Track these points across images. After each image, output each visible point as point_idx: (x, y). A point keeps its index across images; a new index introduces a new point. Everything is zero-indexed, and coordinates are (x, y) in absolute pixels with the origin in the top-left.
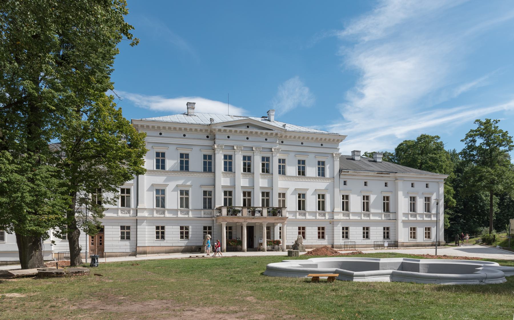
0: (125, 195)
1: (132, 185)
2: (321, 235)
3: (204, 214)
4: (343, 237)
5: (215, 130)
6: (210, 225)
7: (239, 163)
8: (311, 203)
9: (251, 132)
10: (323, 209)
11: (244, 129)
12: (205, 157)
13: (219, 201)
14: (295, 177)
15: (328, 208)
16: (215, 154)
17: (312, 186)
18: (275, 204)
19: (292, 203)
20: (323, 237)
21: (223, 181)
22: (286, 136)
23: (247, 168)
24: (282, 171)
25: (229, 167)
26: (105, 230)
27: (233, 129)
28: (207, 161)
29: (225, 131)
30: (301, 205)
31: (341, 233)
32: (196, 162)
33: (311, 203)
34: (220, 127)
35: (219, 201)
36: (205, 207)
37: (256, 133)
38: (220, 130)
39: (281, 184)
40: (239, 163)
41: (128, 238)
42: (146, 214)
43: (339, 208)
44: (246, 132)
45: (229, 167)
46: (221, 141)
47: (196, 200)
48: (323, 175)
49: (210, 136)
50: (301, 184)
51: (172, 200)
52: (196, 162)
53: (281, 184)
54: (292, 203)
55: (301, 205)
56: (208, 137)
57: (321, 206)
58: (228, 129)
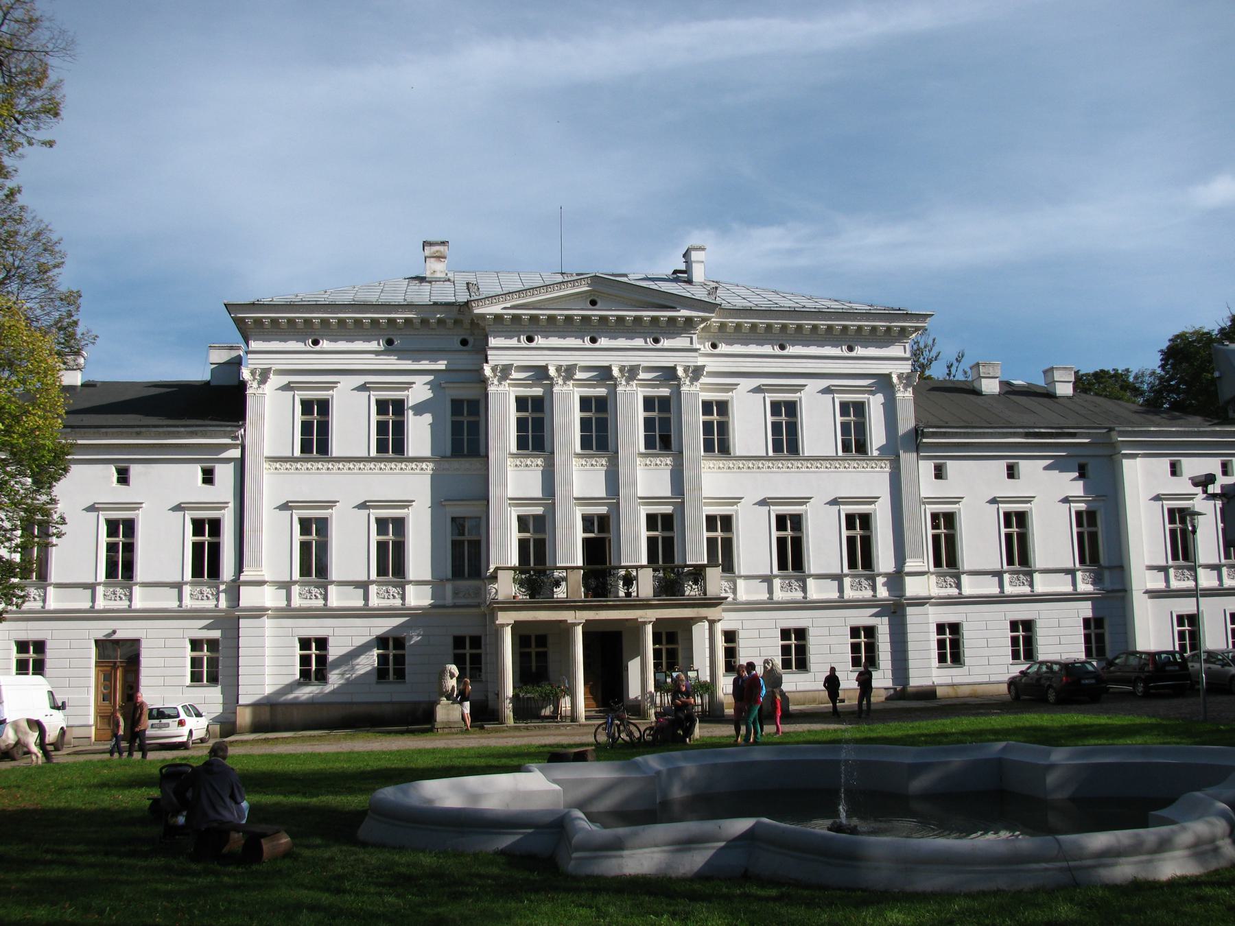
1: (221, 506)
3: (456, 593)
4: (942, 658)
5: (483, 316)
6: (474, 631)
7: (568, 421)
8: (825, 546)
9: (603, 319)
10: (868, 563)
13: (505, 548)
14: (766, 458)
15: (884, 560)
16: (487, 395)
18: (695, 551)
19: (755, 546)
21: (513, 480)
23: (599, 433)
24: (718, 441)
25: (535, 434)
28: (465, 419)
30: (791, 555)
31: (934, 645)
33: (825, 546)
34: (497, 309)
35: (505, 548)
38: (498, 318)
39: (713, 482)
40: (568, 421)
41: (213, 680)
42: (270, 598)
43: (920, 561)
44: (586, 319)
45: (535, 434)
46: (502, 351)
48: (862, 448)
49: (471, 340)
50: (785, 481)
51: (351, 552)
53: (713, 482)
55: (791, 555)
56: (464, 342)
57: (860, 553)
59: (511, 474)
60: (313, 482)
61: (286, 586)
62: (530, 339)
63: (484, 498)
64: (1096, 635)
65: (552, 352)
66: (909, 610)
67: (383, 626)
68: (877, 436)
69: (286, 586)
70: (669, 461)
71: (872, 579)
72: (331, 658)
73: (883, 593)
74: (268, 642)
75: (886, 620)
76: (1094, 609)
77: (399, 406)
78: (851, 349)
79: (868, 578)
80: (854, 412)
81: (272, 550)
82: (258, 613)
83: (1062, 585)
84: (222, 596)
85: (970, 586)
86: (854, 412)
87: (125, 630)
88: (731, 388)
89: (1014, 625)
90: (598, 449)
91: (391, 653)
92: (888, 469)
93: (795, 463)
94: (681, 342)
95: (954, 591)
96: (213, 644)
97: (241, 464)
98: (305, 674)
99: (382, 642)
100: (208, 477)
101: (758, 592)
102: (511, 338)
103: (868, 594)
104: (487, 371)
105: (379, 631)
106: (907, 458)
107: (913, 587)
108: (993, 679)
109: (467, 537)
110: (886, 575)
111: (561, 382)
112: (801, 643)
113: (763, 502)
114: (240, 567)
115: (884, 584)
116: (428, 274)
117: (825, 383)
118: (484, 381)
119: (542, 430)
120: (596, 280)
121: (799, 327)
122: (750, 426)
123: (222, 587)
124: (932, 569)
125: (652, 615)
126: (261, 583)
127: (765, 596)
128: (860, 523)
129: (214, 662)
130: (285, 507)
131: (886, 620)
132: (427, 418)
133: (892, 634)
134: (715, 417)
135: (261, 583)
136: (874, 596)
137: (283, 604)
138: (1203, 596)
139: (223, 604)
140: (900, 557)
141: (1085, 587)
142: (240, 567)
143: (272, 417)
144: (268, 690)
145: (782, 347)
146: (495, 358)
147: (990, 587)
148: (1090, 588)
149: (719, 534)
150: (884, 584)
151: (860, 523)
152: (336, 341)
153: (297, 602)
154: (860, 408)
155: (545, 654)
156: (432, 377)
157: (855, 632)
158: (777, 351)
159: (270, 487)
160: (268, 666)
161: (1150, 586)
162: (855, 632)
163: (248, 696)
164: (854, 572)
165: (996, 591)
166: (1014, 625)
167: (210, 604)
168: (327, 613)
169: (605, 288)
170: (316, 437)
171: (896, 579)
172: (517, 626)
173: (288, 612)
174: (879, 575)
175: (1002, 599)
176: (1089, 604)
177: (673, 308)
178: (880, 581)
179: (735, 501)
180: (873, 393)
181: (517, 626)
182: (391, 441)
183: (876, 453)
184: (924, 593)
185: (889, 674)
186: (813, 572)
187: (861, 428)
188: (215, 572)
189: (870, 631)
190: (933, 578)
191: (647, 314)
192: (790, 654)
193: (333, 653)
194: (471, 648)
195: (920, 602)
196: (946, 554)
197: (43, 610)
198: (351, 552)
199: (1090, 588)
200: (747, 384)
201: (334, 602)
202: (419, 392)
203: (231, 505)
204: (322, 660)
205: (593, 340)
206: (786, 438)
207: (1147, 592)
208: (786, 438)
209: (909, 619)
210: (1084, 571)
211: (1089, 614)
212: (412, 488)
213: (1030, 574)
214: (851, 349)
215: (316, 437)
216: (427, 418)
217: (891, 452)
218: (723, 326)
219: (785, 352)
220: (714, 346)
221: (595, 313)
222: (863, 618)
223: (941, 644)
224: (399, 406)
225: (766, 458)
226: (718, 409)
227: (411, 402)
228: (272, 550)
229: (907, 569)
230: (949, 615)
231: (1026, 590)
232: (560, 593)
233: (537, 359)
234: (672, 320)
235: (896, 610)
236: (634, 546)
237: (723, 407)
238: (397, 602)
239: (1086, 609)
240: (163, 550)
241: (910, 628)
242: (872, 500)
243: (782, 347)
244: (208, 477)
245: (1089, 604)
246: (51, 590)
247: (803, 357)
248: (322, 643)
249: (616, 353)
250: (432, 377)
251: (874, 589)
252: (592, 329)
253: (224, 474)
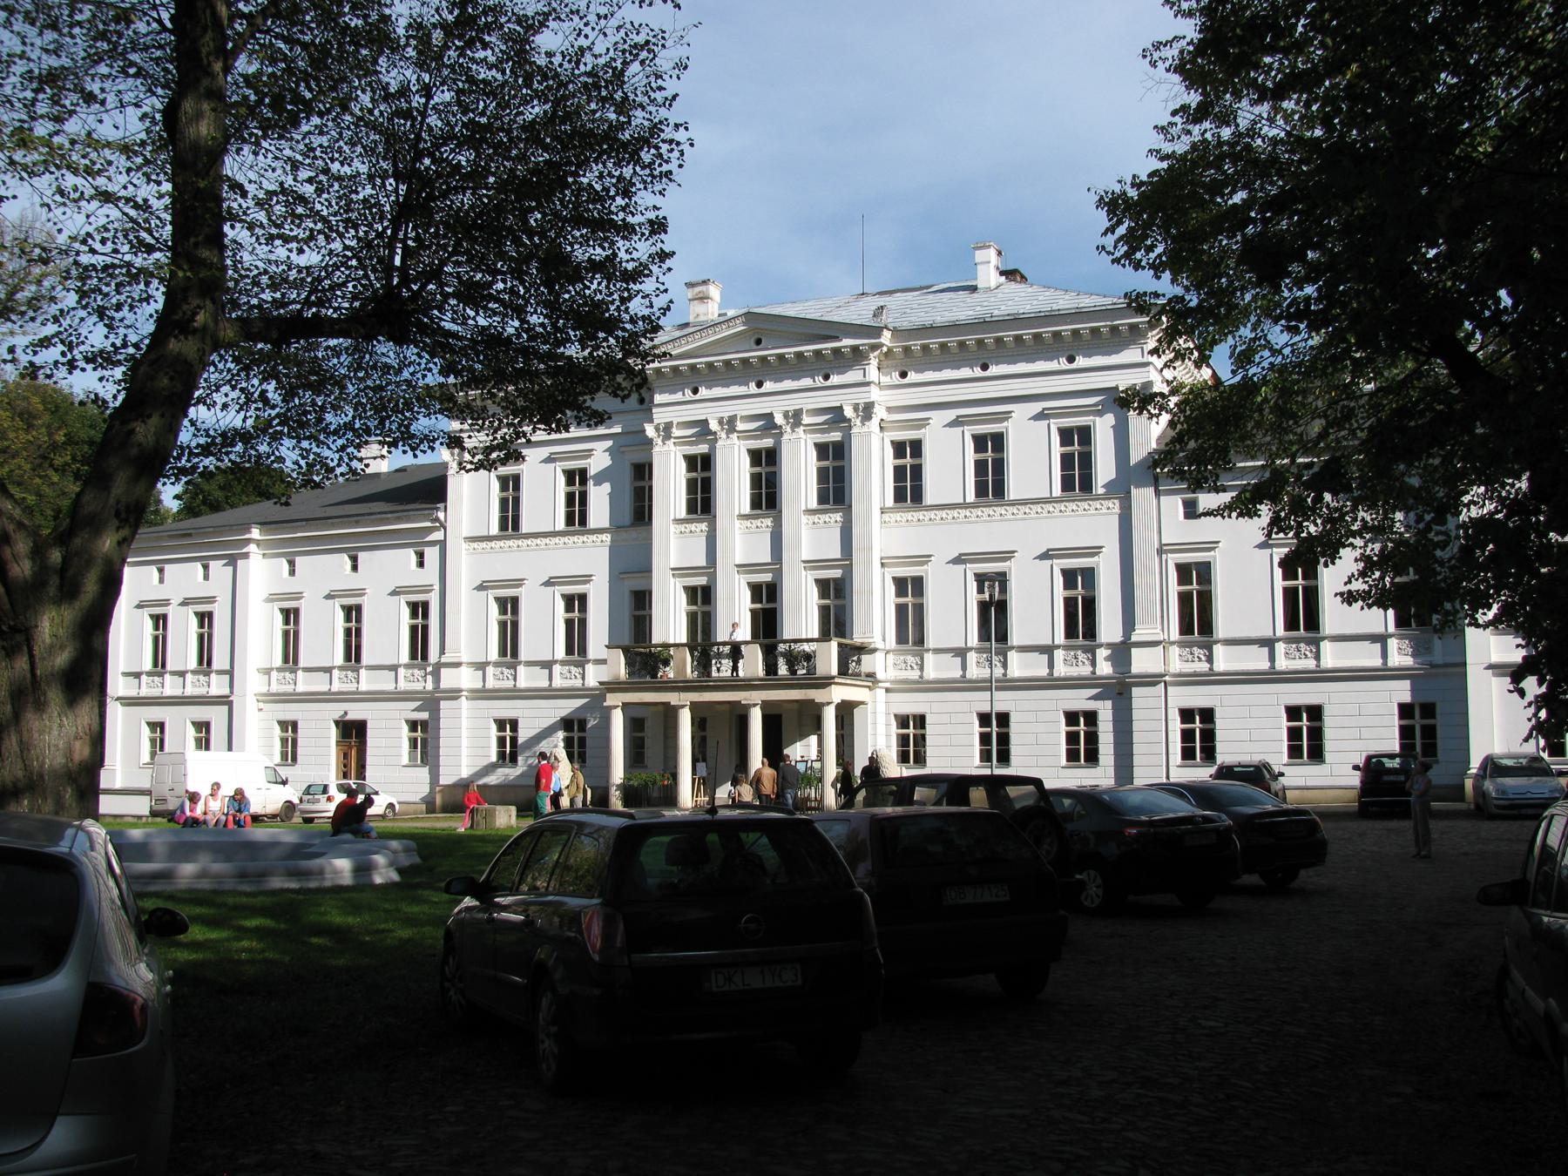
1: (427, 589)
2: (1082, 748)
8: (1036, 611)
10: (1091, 633)
14: (964, 505)
15: (1109, 627)
17: (1038, 534)
19: (951, 613)
20: (1092, 757)
26: (370, 733)
33: (1036, 611)
35: (670, 622)
41: (424, 762)
42: (466, 679)
48: (1087, 485)
57: (1080, 619)
59: (805, 533)
60: (509, 560)
61: (481, 666)
62: (695, 391)
63: (648, 570)
64: (1423, 727)
65: (713, 405)
66: (1136, 691)
67: (567, 707)
68: (1105, 469)
69: (481, 666)
70: (768, 522)
71: (1091, 651)
72: (520, 741)
73: (1105, 669)
74: (465, 723)
75: (1109, 704)
76: (1413, 690)
77: (583, 473)
78: (1071, 359)
79: (1086, 650)
80: (1077, 440)
81: (469, 631)
82: (454, 694)
83: (1368, 657)
84: (429, 678)
85: (1224, 659)
86: (1077, 440)
87: (355, 712)
88: (922, 424)
89: (1293, 712)
90: (835, 502)
91: (576, 735)
92: (1117, 510)
93: (998, 509)
94: (853, 376)
95: (1205, 667)
96: (424, 724)
97: (443, 544)
98: (502, 755)
99: (567, 723)
101: (1035, 667)
102: (674, 392)
103: (1085, 670)
104: (650, 431)
105: (564, 713)
106: (1143, 496)
107: (1142, 661)
108: (1309, 784)
110: (1109, 646)
111: (723, 435)
112: (1316, 724)
113: (959, 560)
114: (442, 651)
115: (1107, 659)
116: (691, 319)
117: (1037, 407)
118: (649, 443)
119: (843, 481)
120: (749, 316)
121: (1056, 334)
122: (949, 466)
123: (429, 669)
124: (1175, 634)
125: (756, 697)
126: (458, 665)
127: (958, 674)
128: (1080, 580)
129: (425, 740)
130: (481, 587)
131: (1109, 704)
132: (607, 487)
133: (1116, 721)
134: (908, 461)
135: (458, 665)
136: (1094, 673)
137: (479, 685)
138: (998, 689)
139: (430, 686)
140: (1129, 622)
141: (1399, 655)
142: (442, 651)
144: (465, 773)
145: (985, 367)
146: (660, 416)
147: (1257, 660)
148: (1408, 661)
149: (909, 600)
150: (1107, 659)
151: (1080, 580)
152: (781, 380)
153: (491, 683)
154: (1085, 434)
155: (923, 737)
156: (610, 443)
157: (1071, 718)
158: (978, 372)
159: (466, 566)
160: (468, 749)
161: (1495, 658)
162: (1071, 718)
163: (446, 779)
164: (1073, 642)
165: (1265, 665)
166: (1293, 712)
167: (418, 686)
168: (515, 694)
169: (760, 327)
171: (1121, 653)
172: (765, 705)
173: (482, 694)
174: (1101, 646)
175: (1272, 677)
176: (1407, 684)
177: (836, 338)
178: (1102, 653)
179: (924, 559)
180: (1100, 413)
181: (626, 706)
182: (577, 514)
183: (1101, 491)
184: (1159, 669)
185: (1111, 772)
186: (1015, 643)
187: (1087, 460)
188: (425, 657)
189: (1091, 717)
190: (1175, 651)
191: (808, 349)
192: (990, 744)
193: (523, 735)
194: (1422, 717)
195: (1151, 680)
196: (1197, 617)
197: (515, 689)
198: (543, 630)
199: (1408, 661)
200: (1022, 412)
201: (522, 683)
202: (599, 460)
203: (437, 587)
204: (514, 740)
205: (759, 385)
206: (991, 481)
207: (1490, 667)
208: (991, 481)
209: (1136, 703)
210: (1401, 637)
211: (1406, 698)
212: (591, 559)
213: (1315, 643)
214: (1071, 359)
216: (607, 487)
217: (1120, 491)
218: (925, 348)
219: (987, 373)
220: (904, 375)
222: (1080, 700)
223: (1187, 736)
224: (583, 473)
225: (964, 505)
226: (907, 451)
227: (592, 472)
228: (469, 631)
229: (1134, 638)
230: (1197, 697)
231: (1310, 664)
232: (670, 673)
233: (696, 412)
234: (836, 351)
235: (1120, 690)
236: (801, 617)
237: (917, 447)
238: (578, 683)
239: (1402, 692)
240: (387, 634)
241: (1136, 715)
242: (1094, 551)
243: (985, 367)
245: (1407, 684)
246: (363, 672)
247: (1008, 379)
248: (514, 724)
249: (780, 398)
250: (610, 443)
251: (1094, 664)
252: (756, 372)
253: (432, 554)
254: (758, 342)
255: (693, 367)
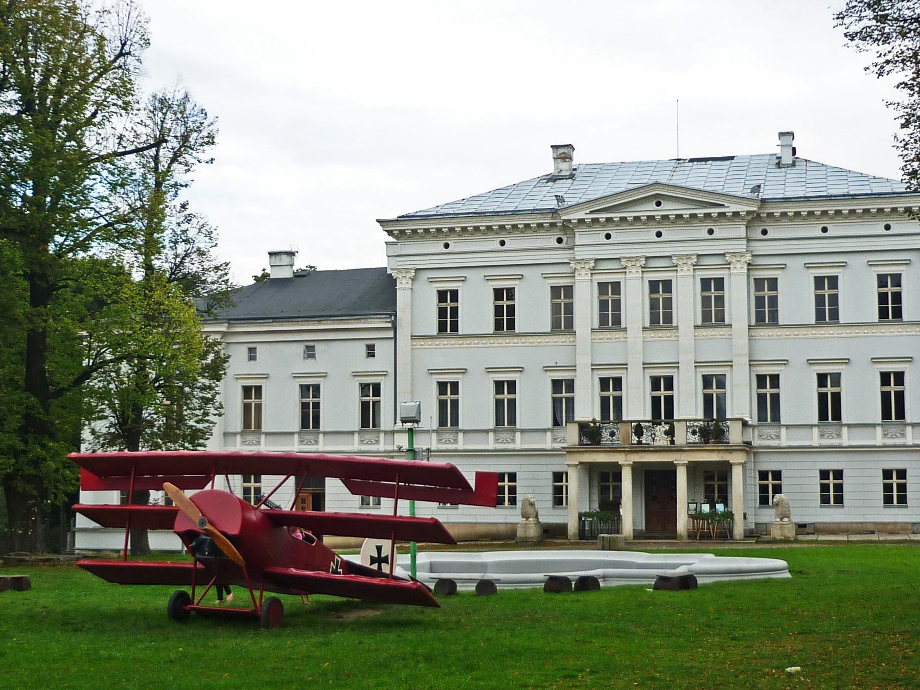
0: (371, 399)
5: (569, 221)
7: (635, 303)
8: (861, 399)
9: (665, 217)
11: (650, 209)
12: (555, 291)
19: (799, 400)
22: (771, 215)
27: (616, 216)
29: (595, 221)
30: (830, 408)
32: (533, 310)
33: (861, 399)
34: (581, 215)
36: (556, 423)
37: (679, 217)
38: (581, 221)
40: (635, 303)
44: (651, 218)
47: (533, 406)
49: (565, 239)
52: (533, 310)
54: (799, 400)
55: (830, 408)
56: (560, 241)
58: (602, 216)
60: (447, 355)
100: (371, 351)
109: (564, 394)
128: (892, 380)
143: (417, 306)
170: (448, 321)
206: (827, 311)
215: (448, 321)
221: (658, 214)
244: (371, 351)
253: (383, 350)
254: (658, 204)
255: (609, 220)
